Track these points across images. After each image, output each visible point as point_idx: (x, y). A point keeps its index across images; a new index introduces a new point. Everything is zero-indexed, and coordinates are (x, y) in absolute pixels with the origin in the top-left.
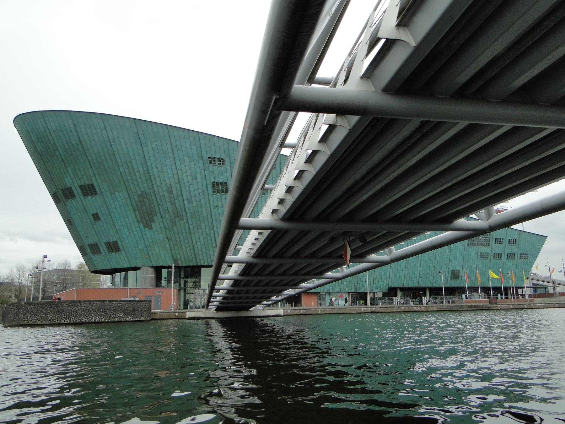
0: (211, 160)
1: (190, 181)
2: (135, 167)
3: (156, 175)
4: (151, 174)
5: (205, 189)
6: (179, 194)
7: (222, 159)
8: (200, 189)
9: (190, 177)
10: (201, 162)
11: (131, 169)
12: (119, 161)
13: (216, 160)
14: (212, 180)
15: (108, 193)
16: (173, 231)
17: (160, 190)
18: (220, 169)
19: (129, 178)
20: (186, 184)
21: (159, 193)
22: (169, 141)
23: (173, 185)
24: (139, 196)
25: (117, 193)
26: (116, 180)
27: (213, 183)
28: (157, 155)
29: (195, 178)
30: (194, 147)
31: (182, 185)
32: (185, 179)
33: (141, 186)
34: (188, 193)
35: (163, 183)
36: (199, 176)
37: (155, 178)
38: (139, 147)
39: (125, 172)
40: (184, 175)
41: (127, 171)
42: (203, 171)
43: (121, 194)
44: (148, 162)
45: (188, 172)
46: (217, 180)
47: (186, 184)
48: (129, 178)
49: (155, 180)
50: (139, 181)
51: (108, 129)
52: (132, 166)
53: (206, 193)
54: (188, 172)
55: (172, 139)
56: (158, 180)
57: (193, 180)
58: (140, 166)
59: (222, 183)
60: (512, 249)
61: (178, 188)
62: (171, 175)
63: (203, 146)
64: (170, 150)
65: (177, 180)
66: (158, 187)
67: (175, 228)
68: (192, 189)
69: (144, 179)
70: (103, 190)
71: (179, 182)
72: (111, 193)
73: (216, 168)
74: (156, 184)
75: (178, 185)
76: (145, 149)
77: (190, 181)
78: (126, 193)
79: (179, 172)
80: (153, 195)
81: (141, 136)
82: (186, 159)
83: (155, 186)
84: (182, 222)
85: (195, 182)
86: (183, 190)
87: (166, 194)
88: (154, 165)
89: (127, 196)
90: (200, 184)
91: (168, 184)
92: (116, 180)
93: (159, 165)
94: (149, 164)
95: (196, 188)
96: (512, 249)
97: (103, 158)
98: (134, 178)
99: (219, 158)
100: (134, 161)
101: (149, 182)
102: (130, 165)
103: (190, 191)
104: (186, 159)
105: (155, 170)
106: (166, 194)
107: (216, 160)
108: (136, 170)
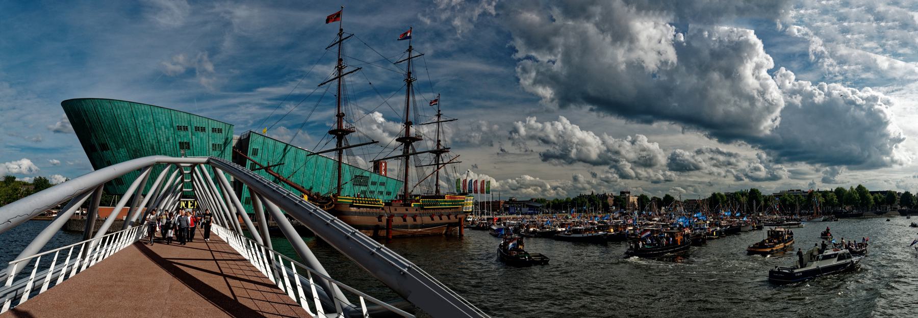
0: (179, 128)
1: (165, 141)
2: (131, 131)
3: (144, 137)
4: (141, 137)
5: (175, 147)
6: (158, 149)
7: (187, 127)
8: (172, 147)
9: (165, 139)
10: (172, 129)
11: (129, 134)
12: (121, 128)
13: (183, 127)
14: (180, 141)
15: (115, 149)
16: (155, 173)
17: (147, 147)
18: (185, 133)
19: (127, 140)
20: (163, 143)
21: (146, 149)
22: (151, 116)
23: (154, 144)
24: (133, 151)
25: (120, 149)
26: (120, 141)
27: (180, 143)
28: (144, 125)
29: (168, 140)
30: (167, 119)
31: (160, 144)
32: (162, 140)
33: (135, 144)
34: (164, 149)
35: (149, 143)
36: (171, 138)
37: (143, 140)
38: (133, 120)
39: (125, 136)
40: (161, 137)
41: (126, 135)
42: (173, 135)
43: (123, 149)
44: (139, 129)
45: (164, 135)
46: (182, 141)
47: (163, 143)
48: (127, 140)
49: (144, 141)
50: (133, 141)
51: (114, 109)
52: (129, 132)
53: (175, 149)
54: (164, 135)
55: (154, 114)
56: (145, 140)
57: (167, 140)
58: (134, 132)
59: (186, 142)
60: (382, 189)
61: (158, 146)
62: (153, 138)
63: (173, 118)
64: (152, 121)
65: (157, 141)
66: (145, 145)
67: (156, 171)
68: (166, 146)
69: (136, 140)
70: (112, 147)
71: (158, 142)
72: (117, 149)
73: (182, 133)
74: (144, 143)
75: (157, 144)
76: (137, 121)
77: (165, 141)
78: (126, 149)
79: (158, 135)
80: (142, 150)
81: (135, 113)
82: (163, 127)
83: (143, 145)
84: (160, 168)
85: (168, 142)
86: (161, 147)
87: (150, 150)
88: (142, 131)
89: (126, 151)
90: (172, 144)
91: (151, 143)
92: (120, 141)
93: (145, 131)
94: (139, 131)
95: (169, 146)
96: (382, 189)
97: (112, 127)
98: (130, 139)
99: (184, 126)
100: (130, 129)
101: (139, 142)
102: (128, 131)
103: (165, 148)
104: (163, 127)
105: (143, 135)
106: (150, 150)
107: (183, 127)
108: (132, 135)
